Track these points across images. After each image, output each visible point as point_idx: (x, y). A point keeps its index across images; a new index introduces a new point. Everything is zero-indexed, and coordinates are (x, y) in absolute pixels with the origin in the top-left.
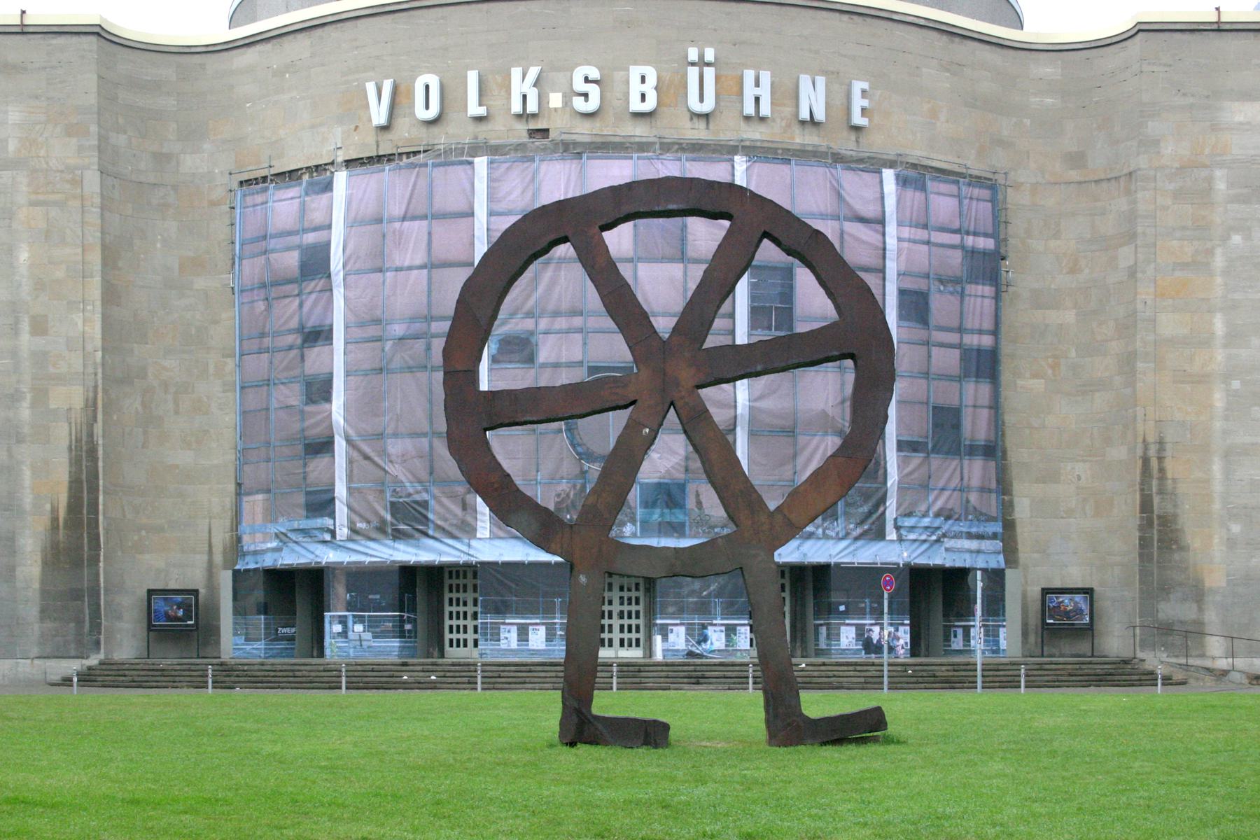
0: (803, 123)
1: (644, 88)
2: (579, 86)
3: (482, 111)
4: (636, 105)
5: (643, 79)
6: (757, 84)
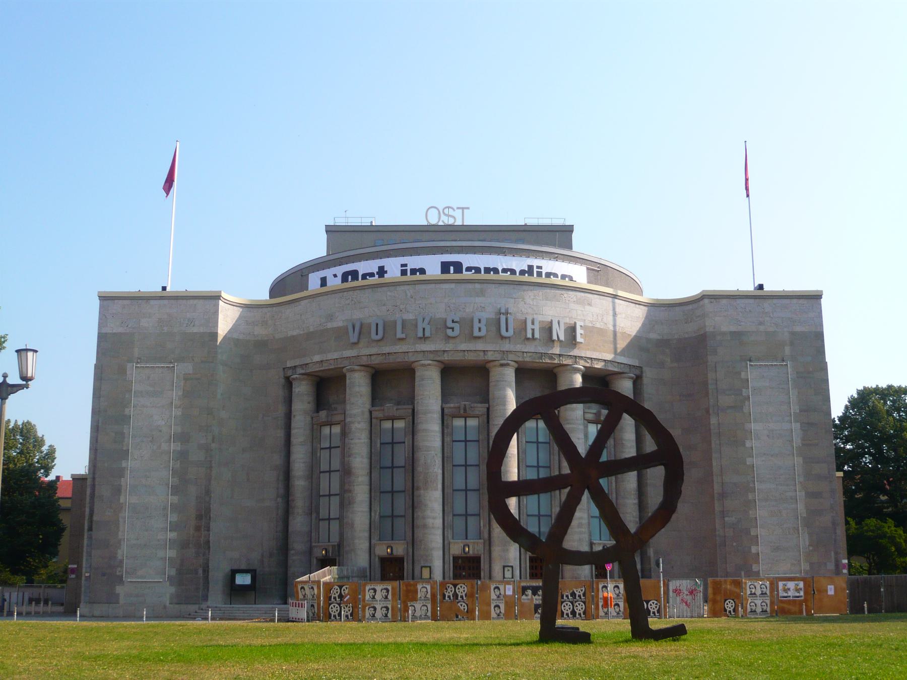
1: (479, 325)
2: (450, 324)
3: (403, 336)
4: (476, 333)
5: (480, 321)
6: (533, 323)
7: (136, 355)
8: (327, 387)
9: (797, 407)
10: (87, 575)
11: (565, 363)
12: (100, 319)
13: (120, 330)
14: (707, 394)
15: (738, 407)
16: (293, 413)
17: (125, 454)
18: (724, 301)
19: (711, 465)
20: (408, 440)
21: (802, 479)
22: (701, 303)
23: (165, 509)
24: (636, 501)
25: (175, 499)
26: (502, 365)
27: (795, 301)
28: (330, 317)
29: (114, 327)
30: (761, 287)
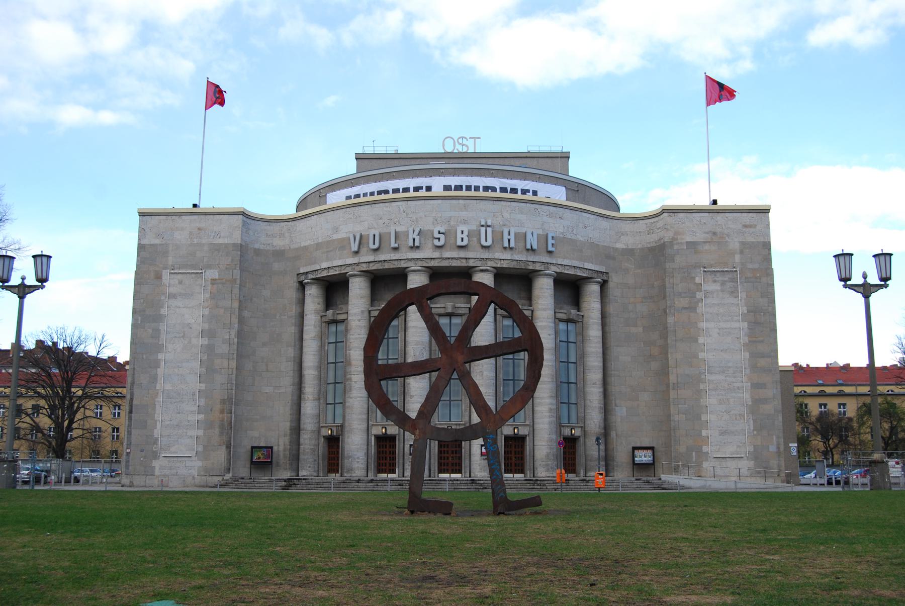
0: (528, 250)
2: (436, 235)
3: (396, 245)
4: (459, 243)
7: (170, 263)
8: (334, 288)
9: (745, 308)
10: (128, 451)
11: (538, 268)
12: (140, 232)
13: (157, 241)
14: (665, 297)
15: (692, 308)
16: (306, 312)
17: (159, 348)
18: (681, 215)
19: (667, 359)
20: (401, 336)
21: (748, 371)
22: (661, 217)
23: (194, 394)
24: (602, 390)
25: (203, 386)
26: (482, 271)
27: (745, 214)
28: (336, 230)
29: (150, 240)
30: (715, 202)
